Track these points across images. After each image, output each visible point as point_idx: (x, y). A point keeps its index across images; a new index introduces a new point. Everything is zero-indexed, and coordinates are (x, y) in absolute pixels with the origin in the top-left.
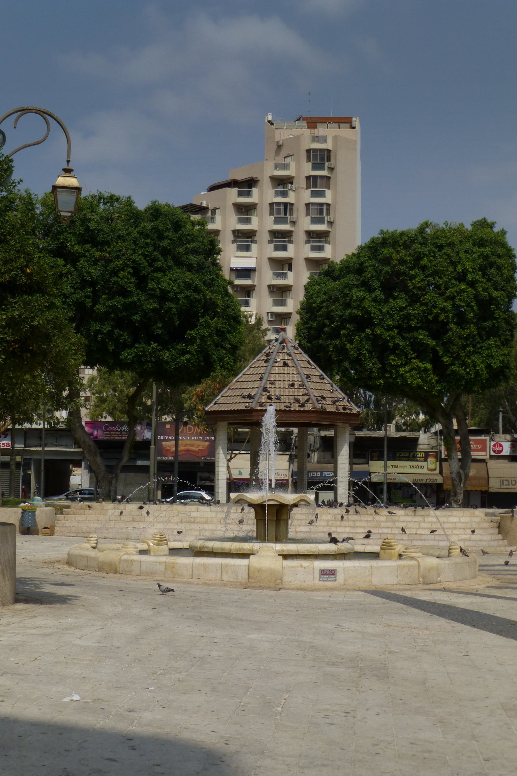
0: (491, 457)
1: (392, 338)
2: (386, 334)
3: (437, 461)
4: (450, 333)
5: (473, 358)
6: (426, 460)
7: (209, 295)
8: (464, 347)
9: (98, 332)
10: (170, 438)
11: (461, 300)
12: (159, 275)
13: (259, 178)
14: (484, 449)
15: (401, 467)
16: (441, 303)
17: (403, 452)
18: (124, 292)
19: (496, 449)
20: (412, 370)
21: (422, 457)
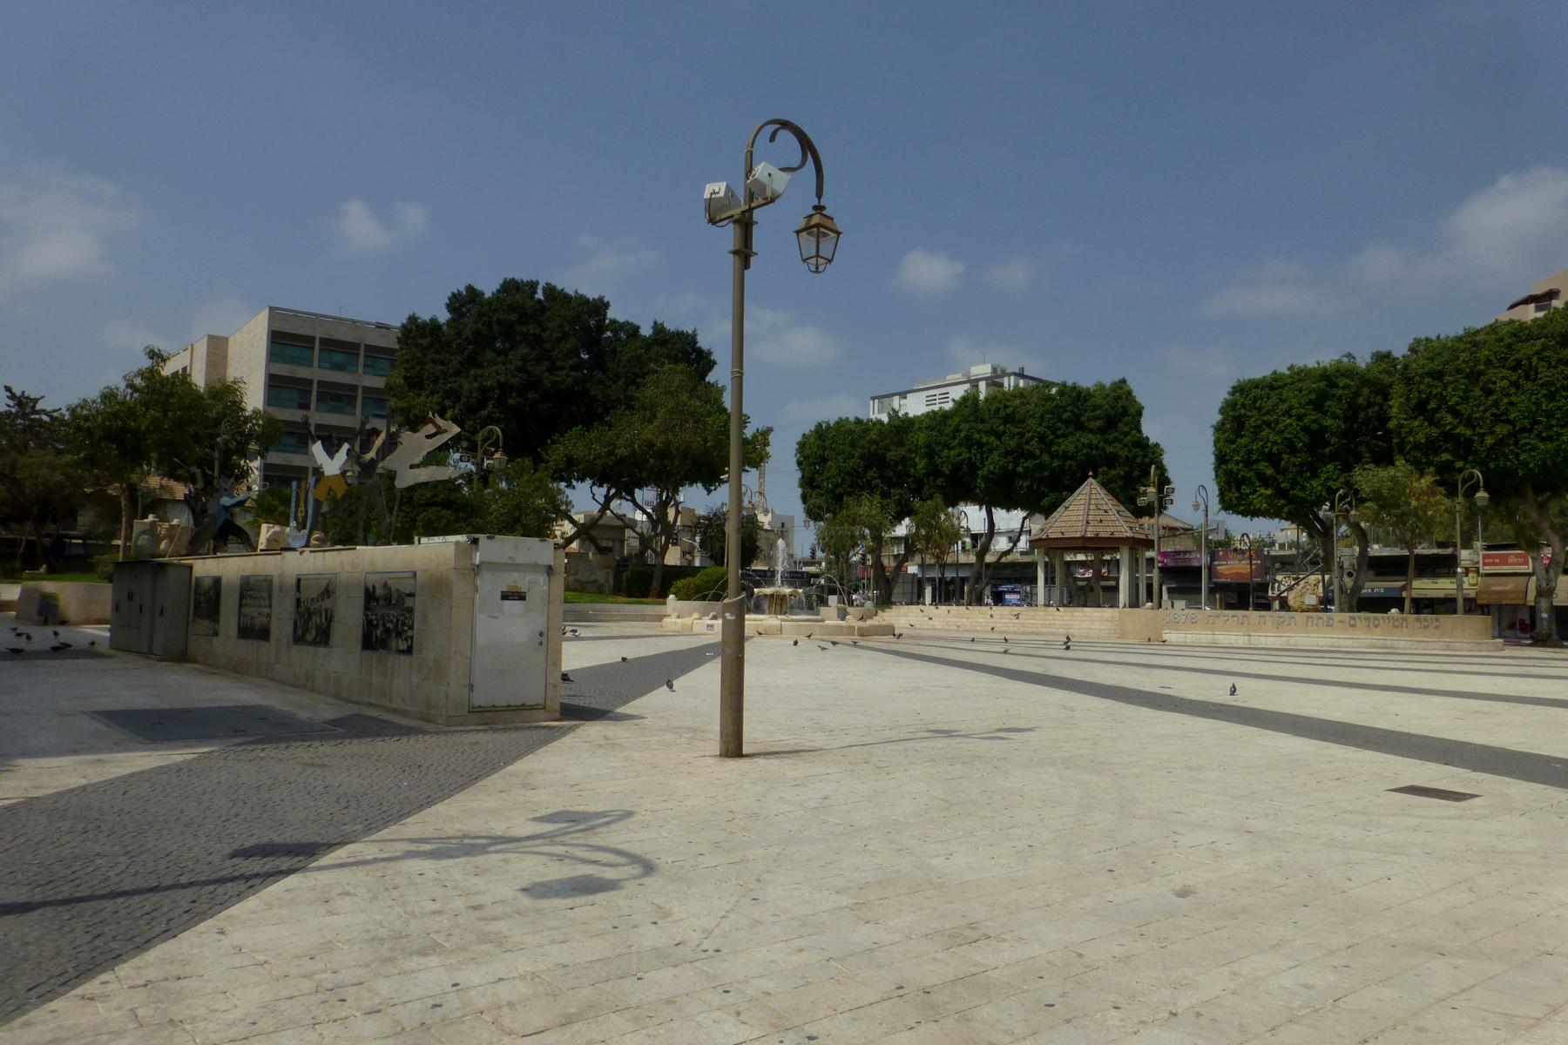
1: (1239, 471)
2: (1235, 468)
4: (1283, 463)
5: (1313, 482)
6: (1467, 576)
7: (1109, 449)
8: (1301, 474)
9: (1021, 487)
11: (1289, 433)
13: (1560, 289)
16: (1272, 437)
18: (1032, 456)
20: (1258, 497)
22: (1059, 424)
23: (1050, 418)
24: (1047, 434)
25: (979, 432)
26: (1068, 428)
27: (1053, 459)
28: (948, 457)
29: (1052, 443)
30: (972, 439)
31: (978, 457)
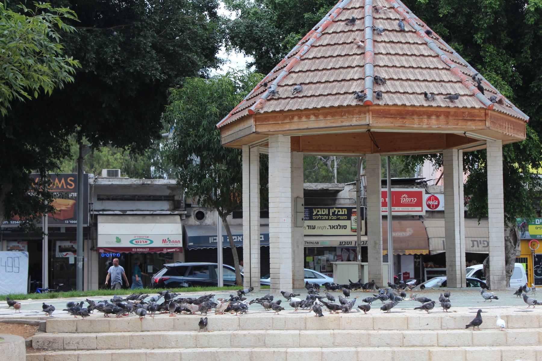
0: (427, 211)
3: (363, 219)
6: (349, 219)
14: (419, 204)
15: (319, 228)
17: (321, 208)
19: (431, 203)
21: (345, 215)
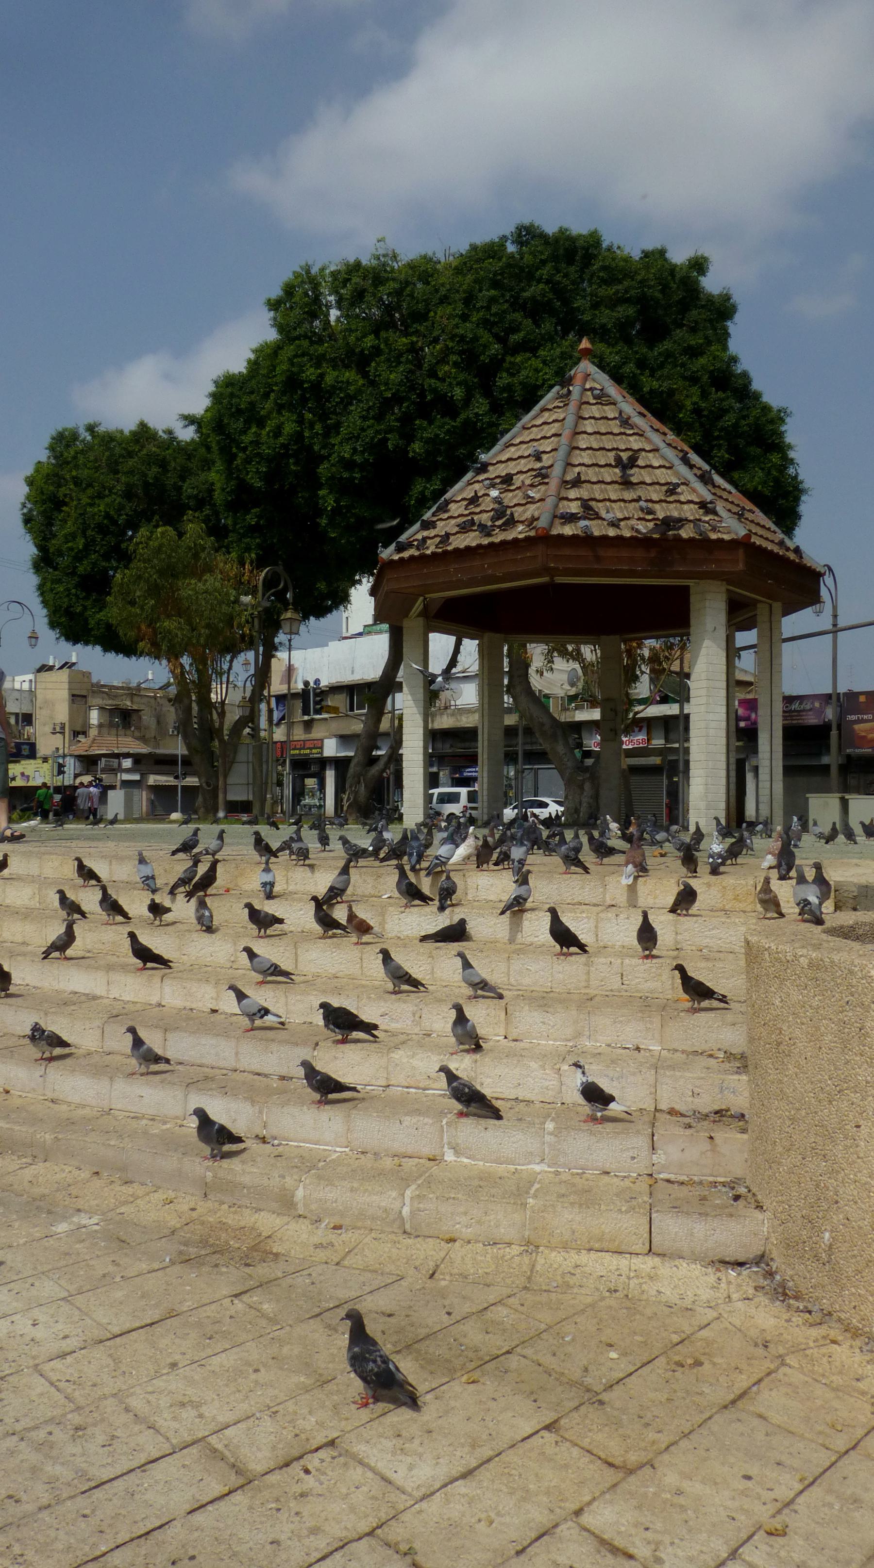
10: (865, 717)
12: (518, 359)
22: (518, 316)
23: (492, 300)
24: (482, 341)
25: (318, 361)
26: (537, 325)
27: (502, 414)
28: (257, 443)
29: (496, 364)
30: (303, 382)
31: (318, 427)
